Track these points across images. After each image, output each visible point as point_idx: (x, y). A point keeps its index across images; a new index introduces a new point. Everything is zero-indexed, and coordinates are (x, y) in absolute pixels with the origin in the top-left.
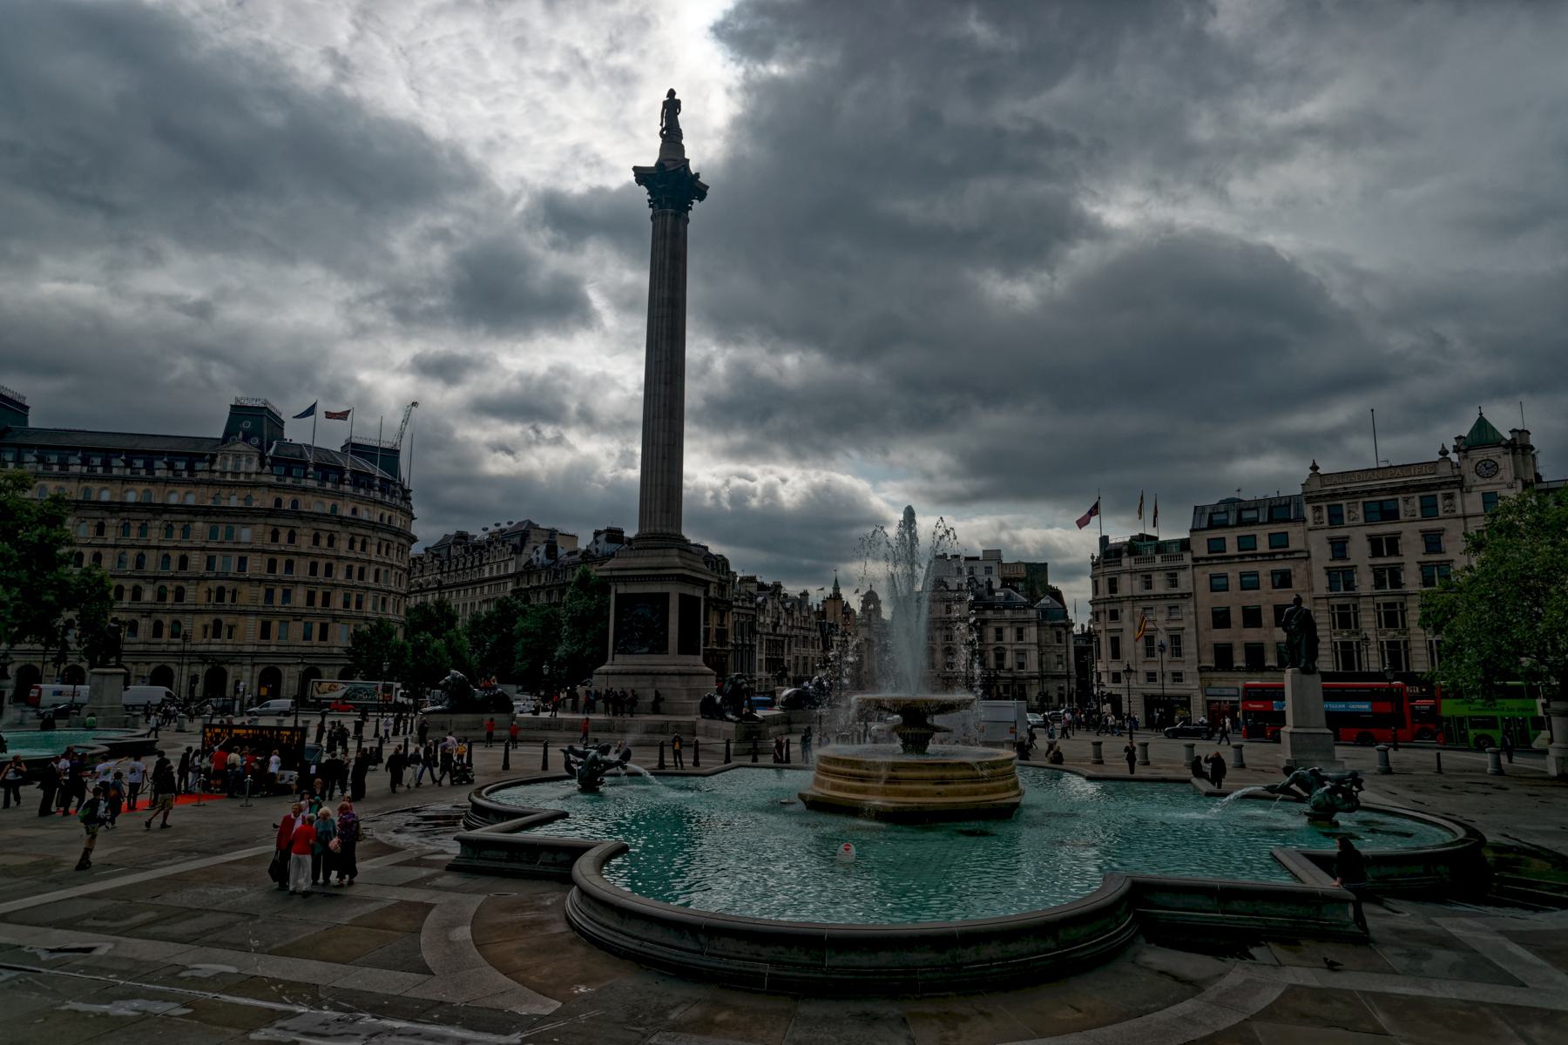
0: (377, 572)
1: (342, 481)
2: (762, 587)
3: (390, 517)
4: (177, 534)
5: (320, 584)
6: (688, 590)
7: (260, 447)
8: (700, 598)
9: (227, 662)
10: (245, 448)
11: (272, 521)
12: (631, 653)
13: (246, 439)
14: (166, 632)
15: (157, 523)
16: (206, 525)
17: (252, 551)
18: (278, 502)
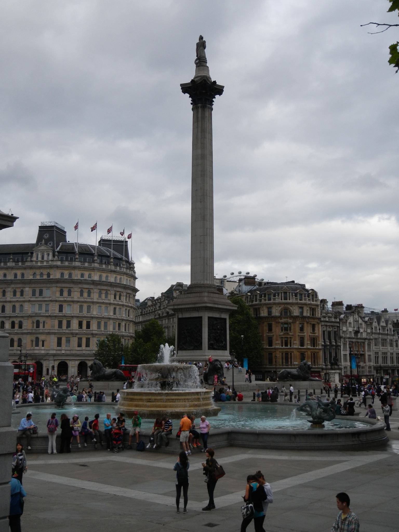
0: (115, 309)
1: (93, 261)
2: (349, 307)
3: (121, 279)
4: (18, 294)
5: (85, 317)
6: (211, 315)
7: (53, 247)
8: (225, 319)
9: (42, 359)
10: (46, 248)
11: (59, 285)
12: (185, 349)
13: (46, 244)
14: (16, 344)
15: (9, 289)
16: (30, 289)
17: (51, 301)
18: (62, 274)
